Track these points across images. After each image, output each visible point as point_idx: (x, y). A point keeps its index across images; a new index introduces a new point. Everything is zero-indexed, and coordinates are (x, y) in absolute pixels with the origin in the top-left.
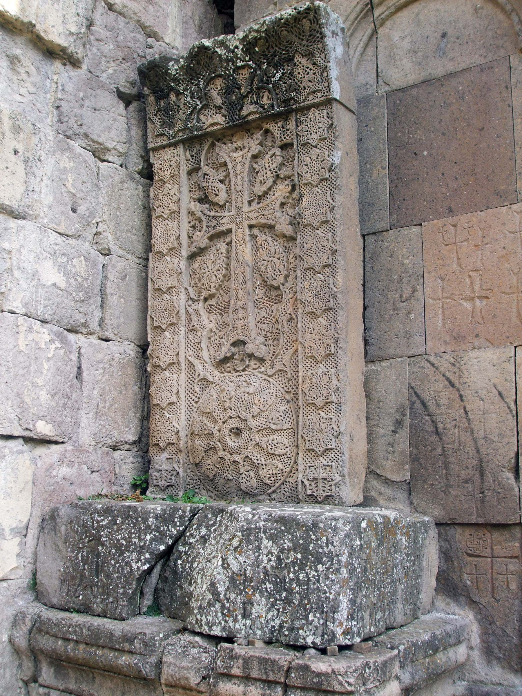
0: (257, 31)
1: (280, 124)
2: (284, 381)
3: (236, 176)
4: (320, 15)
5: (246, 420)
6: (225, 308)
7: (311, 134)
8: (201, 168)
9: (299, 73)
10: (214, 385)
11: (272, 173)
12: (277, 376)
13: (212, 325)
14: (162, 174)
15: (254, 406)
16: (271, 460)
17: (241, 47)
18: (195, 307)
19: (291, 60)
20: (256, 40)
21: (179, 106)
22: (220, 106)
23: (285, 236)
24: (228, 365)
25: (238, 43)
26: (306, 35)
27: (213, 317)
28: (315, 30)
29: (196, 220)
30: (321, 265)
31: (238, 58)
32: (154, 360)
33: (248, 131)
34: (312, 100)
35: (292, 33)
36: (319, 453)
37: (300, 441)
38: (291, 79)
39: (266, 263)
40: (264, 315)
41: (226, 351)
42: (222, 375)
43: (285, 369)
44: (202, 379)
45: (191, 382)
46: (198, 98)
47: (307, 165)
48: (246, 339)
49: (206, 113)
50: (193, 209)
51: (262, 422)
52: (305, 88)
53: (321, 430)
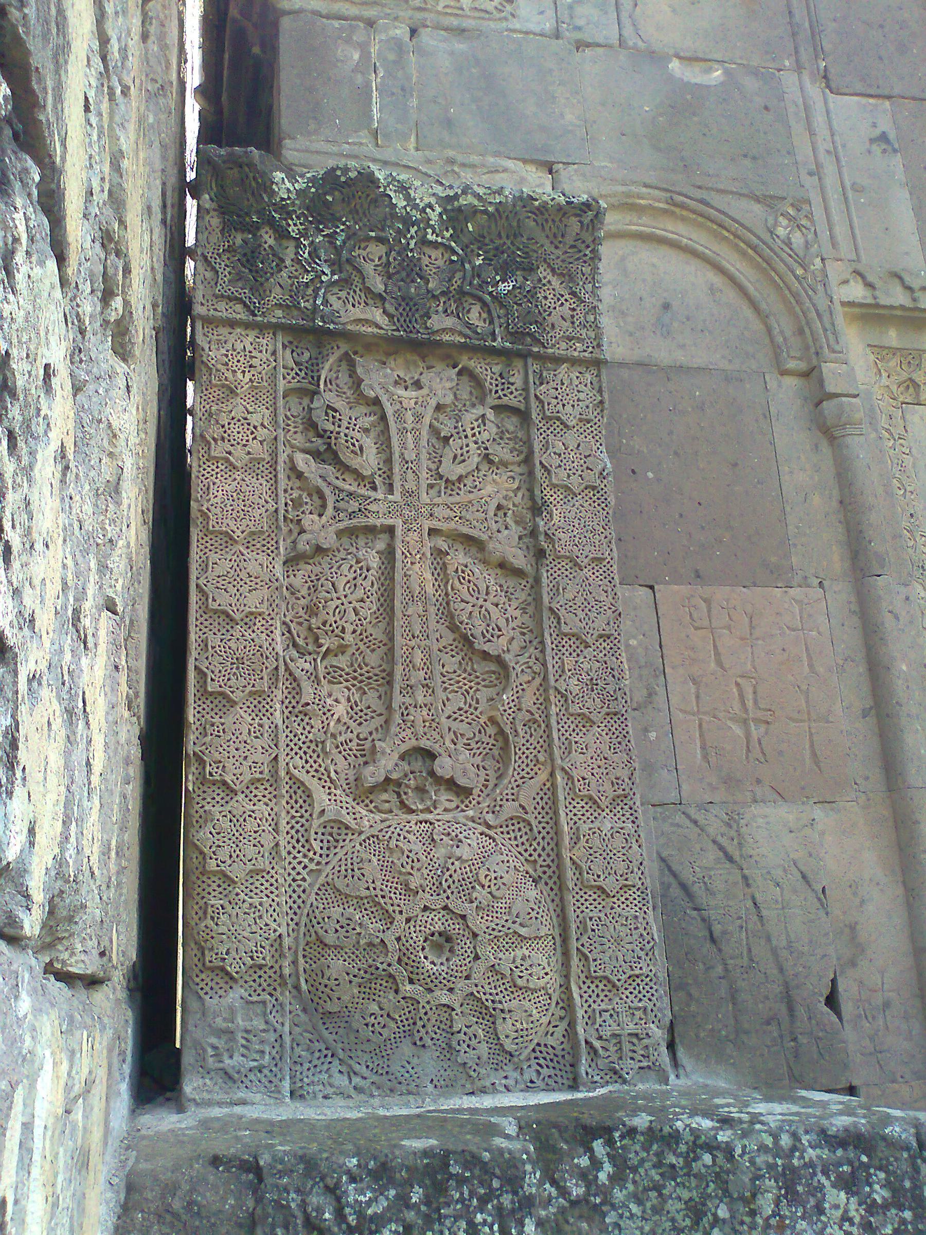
0: (478, 197)
1: (497, 369)
2: (520, 840)
3: (403, 431)
4: (602, 223)
5: (463, 917)
6: (369, 678)
8: (316, 393)
11: (479, 448)
12: (505, 829)
13: (341, 710)
14: (229, 375)
17: (438, 210)
18: (307, 666)
21: (283, 261)
23: (502, 565)
24: (385, 796)
25: (433, 200)
26: (565, 244)
27: (339, 691)
29: (299, 488)
30: (596, 634)
31: (429, 226)
32: (208, 769)
34: (561, 349)
37: (575, 960)
38: (529, 301)
39: (469, 608)
40: (462, 705)
41: (390, 768)
42: (378, 817)
44: (330, 821)
45: (298, 826)
46: (326, 261)
47: (560, 455)
48: (436, 748)
49: (343, 294)
51: (498, 921)
52: (553, 325)
53: (618, 940)
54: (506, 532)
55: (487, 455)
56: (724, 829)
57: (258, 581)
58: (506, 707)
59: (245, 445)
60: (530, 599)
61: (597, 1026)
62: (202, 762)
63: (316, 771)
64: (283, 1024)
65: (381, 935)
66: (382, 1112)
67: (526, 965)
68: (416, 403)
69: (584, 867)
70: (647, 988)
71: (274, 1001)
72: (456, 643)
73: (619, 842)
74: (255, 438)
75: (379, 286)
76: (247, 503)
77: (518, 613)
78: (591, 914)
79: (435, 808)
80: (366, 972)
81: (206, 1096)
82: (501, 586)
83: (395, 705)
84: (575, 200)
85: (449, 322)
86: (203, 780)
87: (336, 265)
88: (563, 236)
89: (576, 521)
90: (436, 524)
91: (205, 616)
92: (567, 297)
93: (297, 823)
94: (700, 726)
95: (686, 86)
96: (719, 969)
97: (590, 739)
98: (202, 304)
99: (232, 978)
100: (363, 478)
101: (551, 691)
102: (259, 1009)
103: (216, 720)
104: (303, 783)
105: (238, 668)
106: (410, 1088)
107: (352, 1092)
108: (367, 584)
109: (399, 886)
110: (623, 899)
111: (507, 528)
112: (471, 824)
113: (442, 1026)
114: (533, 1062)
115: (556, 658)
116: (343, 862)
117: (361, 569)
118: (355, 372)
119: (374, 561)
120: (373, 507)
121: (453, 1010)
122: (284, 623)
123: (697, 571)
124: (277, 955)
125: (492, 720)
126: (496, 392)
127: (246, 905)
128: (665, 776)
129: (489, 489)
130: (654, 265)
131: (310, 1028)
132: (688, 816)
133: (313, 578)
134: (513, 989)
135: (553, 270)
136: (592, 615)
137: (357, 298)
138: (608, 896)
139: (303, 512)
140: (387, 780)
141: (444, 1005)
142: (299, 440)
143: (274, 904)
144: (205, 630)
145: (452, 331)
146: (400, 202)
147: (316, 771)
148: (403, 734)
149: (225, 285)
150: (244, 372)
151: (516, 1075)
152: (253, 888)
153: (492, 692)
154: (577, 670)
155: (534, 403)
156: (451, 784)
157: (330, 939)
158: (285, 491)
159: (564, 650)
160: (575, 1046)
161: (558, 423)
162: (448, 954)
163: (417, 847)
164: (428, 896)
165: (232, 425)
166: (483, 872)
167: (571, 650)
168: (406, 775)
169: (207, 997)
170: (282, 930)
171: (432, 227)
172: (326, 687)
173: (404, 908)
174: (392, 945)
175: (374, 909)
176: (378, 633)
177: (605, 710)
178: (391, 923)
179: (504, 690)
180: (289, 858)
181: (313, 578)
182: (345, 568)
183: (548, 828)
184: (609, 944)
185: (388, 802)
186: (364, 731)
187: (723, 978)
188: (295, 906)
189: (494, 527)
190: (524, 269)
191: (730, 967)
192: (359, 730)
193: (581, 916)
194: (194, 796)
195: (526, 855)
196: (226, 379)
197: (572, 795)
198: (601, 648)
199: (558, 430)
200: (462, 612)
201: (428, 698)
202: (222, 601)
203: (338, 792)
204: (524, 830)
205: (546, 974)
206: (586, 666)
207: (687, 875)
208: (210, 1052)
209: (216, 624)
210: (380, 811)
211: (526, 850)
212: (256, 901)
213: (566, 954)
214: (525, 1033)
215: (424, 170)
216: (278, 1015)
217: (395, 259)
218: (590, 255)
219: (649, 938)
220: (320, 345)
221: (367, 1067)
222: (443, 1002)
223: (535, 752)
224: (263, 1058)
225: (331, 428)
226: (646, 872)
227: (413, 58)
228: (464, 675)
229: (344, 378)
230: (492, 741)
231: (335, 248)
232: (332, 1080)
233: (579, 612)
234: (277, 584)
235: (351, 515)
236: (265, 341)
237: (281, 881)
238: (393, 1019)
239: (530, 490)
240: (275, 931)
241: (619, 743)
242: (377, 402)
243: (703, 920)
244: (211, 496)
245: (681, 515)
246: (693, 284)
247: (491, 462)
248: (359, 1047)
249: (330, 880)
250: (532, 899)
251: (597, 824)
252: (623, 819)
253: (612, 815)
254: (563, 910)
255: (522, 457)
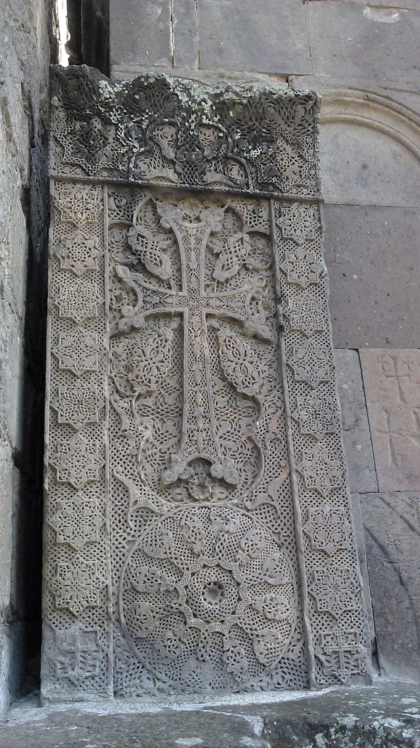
1: (250, 208)
2: (269, 519)
4: (319, 109)
5: (230, 572)
6: (168, 412)
7: (295, 230)
8: (132, 226)
9: (282, 160)
10: (163, 518)
11: (239, 260)
12: (258, 511)
13: (148, 434)
14: (72, 215)
15: (240, 551)
16: (267, 629)
17: (210, 103)
18: (125, 405)
19: (272, 141)
20: (234, 103)
22: (172, 160)
23: (255, 337)
24: (178, 490)
25: (206, 97)
26: (295, 123)
27: (148, 421)
28: (307, 122)
29: (120, 289)
30: (318, 380)
32: (58, 474)
33: (202, 202)
35: (280, 114)
36: (337, 617)
37: (307, 601)
38: (271, 162)
40: (229, 429)
41: (181, 471)
43: (272, 503)
44: (141, 508)
46: (136, 139)
47: (293, 263)
48: (212, 458)
49: (148, 160)
50: (121, 274)
51: (254, 574)
52: (287, 177)
54: (257, 315)
55: (244, 265)
56: (408, 509)
57: (92, 349)
58: (259, 430)
59: (83, 261)
60: (274, 358)
61: (322, 646)
62: (54, 470)
63: (132, 474)
64: (108, 647)
65: (174, 584)
66: (176, 707)
67: (273, 604)
68: (197, 231)
69: (312, 537)
70: (357, 619)
71: (102, 631)
72: (225, 389)
73: (335, 519)
74: (90, 256)
75: (171, 154)
76: (84, 298)
77: (266, 368)
78: (317, 569)
79: (212, 498)
80: (164, 610)
81: (56, 696)
82: (255, 350)
83: (184, 430)
84: (301, 94)
85: (219, 177)
86: (56, 483)
87: (142, 141)
88: (293, 118)
89: (304, 307)
90: (210, 310)
91: (57, 374)
92: (297, 158)
93: (119, 509)
94: (391, 440)
95: (375, 24)
96: (407, 603)
97: (315, 450)
98: (54, 169)
99: (74, 615)
100: (163, 281)
101: (289, 420)
102: (92, 636)
103: (65, 442)
104: (122, 483)
105: (78, 407)
106: (195, 689)
107: (156, 692)
108: (166, 350)
109: (187, 551)
110: (339, 558)
111: (258, 312)
112: (236, 508)
113: (217, 647)
114: (280, 670)
115: (292, 397)
116: (150, 535)
117: (161, 341)
118: (156, 212)
119: (170, 335)
120: (169, 300)
121: (224, 635)
122: (110, 377)
123: (387, 339)
124: (104, 599)
125: (249, 438)
126: (251, 223)
127: (84, 566)
128: (368, 474)
129: (246, 287)
130: (356, 140)
131: (128, 649)
132: (383, 500)
133: (130, 347)
134: (265, 621)
135: (287, 141)
136: (315, 368)
137: (157, 162)
138: (328, 556)
139: (122, 305)
140: (180, 480)
141: (218, 632)
142: (120, 257)
143: (103, 564)
144: (57, 383)
145: (220, 183)
146: (184, 98)
147: (132, 474)
148: (190, 449)
149: (68, 157)
150: (82, 213)
151: (268, 679)
152: (88, 553)
153: (249, 420)
154: (305, 406)
155: (275, 230)
156: (222, 482)
157: (140, 588)
158: (111, 290)
159: (297, 392)
160: (308, 659)
161: (291, 242)
162: (220, 597)
163: (200, 525)
164: (206, 558)
165: (74, 248)
166: (243, 541)
167: (301, 392)
168: (192, 476)
169: (57, 629)
170: (109, 582)
171: (206, 115)
172: (138, 419)
173: (190, 567)
174: (182, 592)
175: (170, 567)
176: (173, 383)
177: (325, 431)
178: (182, 576)
179: (257, 418)
180: (114, 533)
181: (130, 347)
182: (151, 340)
183: (288, 511)
184: (330, 589)
185: (181, 494)
186: (164, 447)
187: (409, 608)
188: (118, 565)
189: (250, 312)
190: (267, 141)
191: (414, 601)
192: (161, 446)
193: (310, 570)
194: (49, 493)
195: (273, 529)
196: (70, 218)
197: (303, 489)
198: (322, 390)
199: (292, 246)
200: (229, 368)
201: (207, 425)
202: (68, 363)
203: (146, 488)
204: (271, 512)
205: (287, 610)
206: (312, 402)
207: (384, 540)
208: (59, 666)
209: (64, 379)
210: (176, 501)
211: (273, 526)
212: (90, 563)
213: (301, 596)
214: (273, 650)
215: (204, 82)
216: (105, 640)
217: (181, 136)
218: (311, 130)
219: (356, 585)
220: (133, 195)
221: (166, 675)
222: (217, 630)
223: (278, 460)
224: (94, 670)
225: (141, 248)
226: (355, 539)
227: (196, 11)
228: (230, 410)
229: (150, 216)
230: (249, 453)
231: (142, 130)
232: (142, 684)
233: (307, 366)
234: (105, 352)
235: (154, 306)
236: (96, 193)
237: (107, 548)
238: (183, 643)
239: (274, 287)
240: (103, 583)
241: (335, 453)
242: (171, 231)
243: (395, 570)
244: (61, 294)
245: (376, 303)
246: (382, 152)
247: (247, 269)
248: (161, 661)
249: (141, 548)
250: (277, 559)
251: (320, 507)
252: (338, 504)
253: (330, 501)
254: (298, 566)
255: (268, 265)
